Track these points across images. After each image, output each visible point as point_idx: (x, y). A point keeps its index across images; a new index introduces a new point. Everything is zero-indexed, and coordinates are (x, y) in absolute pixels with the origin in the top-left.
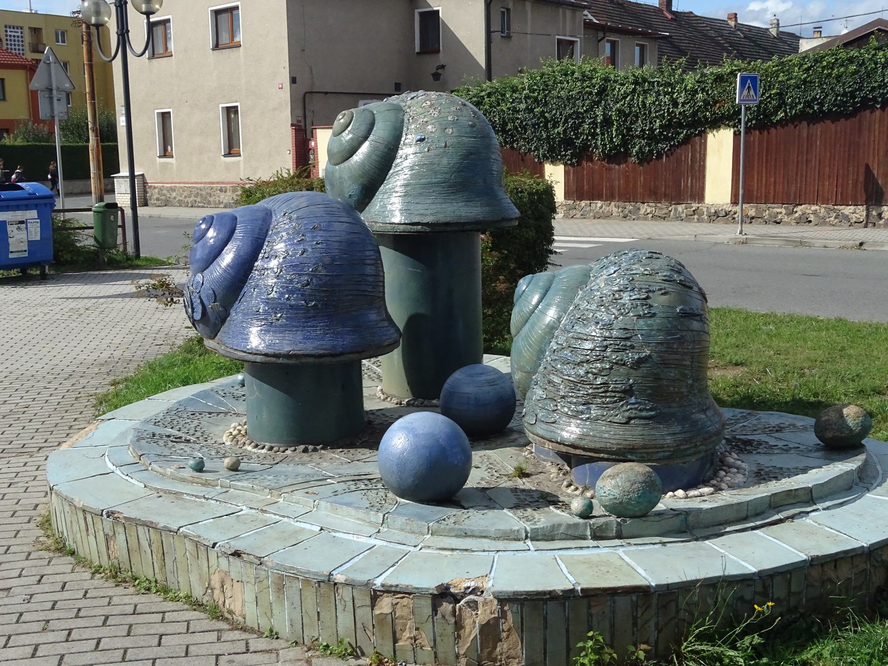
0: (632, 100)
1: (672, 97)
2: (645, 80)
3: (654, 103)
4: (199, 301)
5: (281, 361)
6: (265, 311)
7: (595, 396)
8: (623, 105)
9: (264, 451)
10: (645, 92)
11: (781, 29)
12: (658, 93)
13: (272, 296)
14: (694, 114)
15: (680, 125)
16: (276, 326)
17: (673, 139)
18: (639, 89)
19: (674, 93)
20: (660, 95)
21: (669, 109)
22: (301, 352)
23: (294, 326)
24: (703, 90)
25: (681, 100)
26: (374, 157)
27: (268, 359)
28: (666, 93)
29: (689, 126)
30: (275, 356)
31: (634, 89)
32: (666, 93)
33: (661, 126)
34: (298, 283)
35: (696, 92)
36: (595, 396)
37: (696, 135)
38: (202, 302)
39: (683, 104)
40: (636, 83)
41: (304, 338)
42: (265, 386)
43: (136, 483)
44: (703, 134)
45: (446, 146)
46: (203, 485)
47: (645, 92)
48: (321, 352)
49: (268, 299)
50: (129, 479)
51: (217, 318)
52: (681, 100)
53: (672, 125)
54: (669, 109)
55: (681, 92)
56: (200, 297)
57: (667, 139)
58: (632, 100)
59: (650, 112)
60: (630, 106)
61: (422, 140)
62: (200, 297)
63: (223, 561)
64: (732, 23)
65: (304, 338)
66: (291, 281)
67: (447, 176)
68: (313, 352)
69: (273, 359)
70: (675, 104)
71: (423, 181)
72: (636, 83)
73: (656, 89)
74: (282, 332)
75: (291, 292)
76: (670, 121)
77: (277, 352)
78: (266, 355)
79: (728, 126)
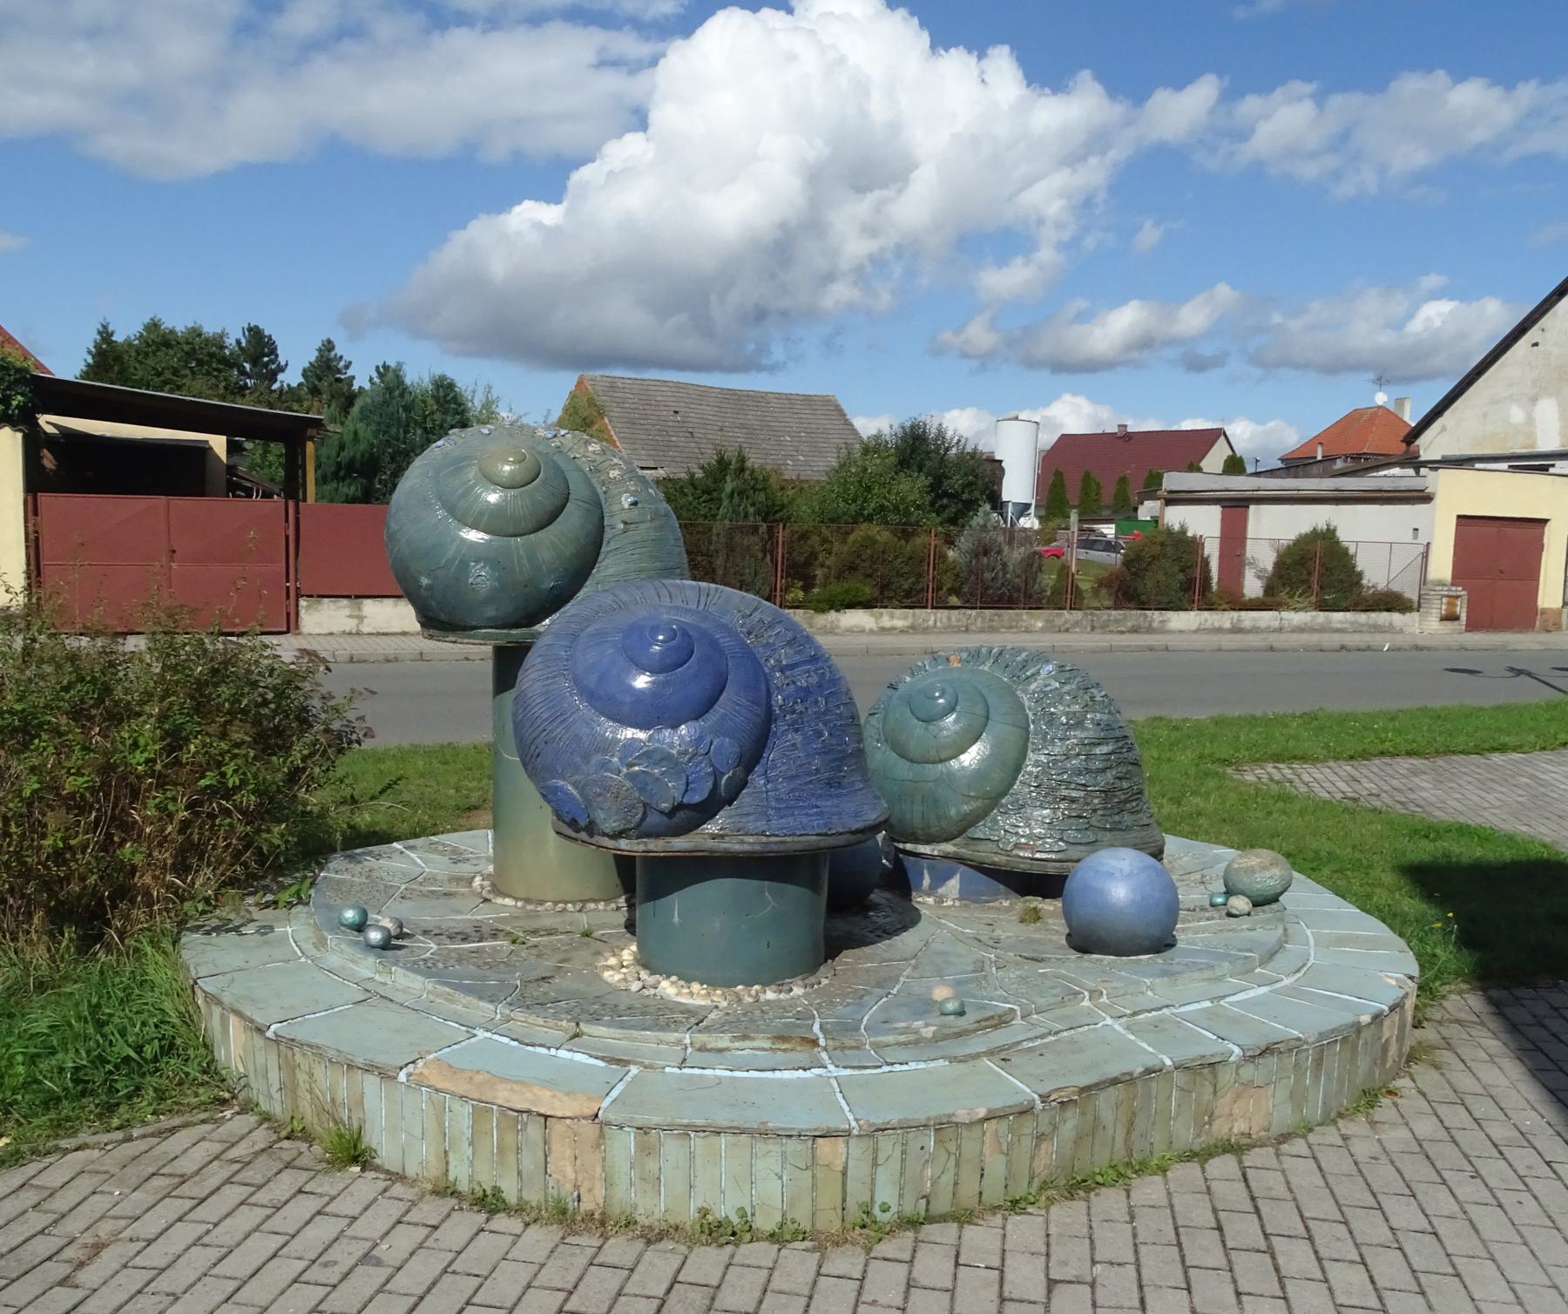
7: (1126, 801)
9: (798, 991)
36: (1126, 801)
43: (922, 1065)
46: (995, 1027)
50: (897, 1068)
61: (635, 504)
63: (1248, 1072)
78: (853, 833)
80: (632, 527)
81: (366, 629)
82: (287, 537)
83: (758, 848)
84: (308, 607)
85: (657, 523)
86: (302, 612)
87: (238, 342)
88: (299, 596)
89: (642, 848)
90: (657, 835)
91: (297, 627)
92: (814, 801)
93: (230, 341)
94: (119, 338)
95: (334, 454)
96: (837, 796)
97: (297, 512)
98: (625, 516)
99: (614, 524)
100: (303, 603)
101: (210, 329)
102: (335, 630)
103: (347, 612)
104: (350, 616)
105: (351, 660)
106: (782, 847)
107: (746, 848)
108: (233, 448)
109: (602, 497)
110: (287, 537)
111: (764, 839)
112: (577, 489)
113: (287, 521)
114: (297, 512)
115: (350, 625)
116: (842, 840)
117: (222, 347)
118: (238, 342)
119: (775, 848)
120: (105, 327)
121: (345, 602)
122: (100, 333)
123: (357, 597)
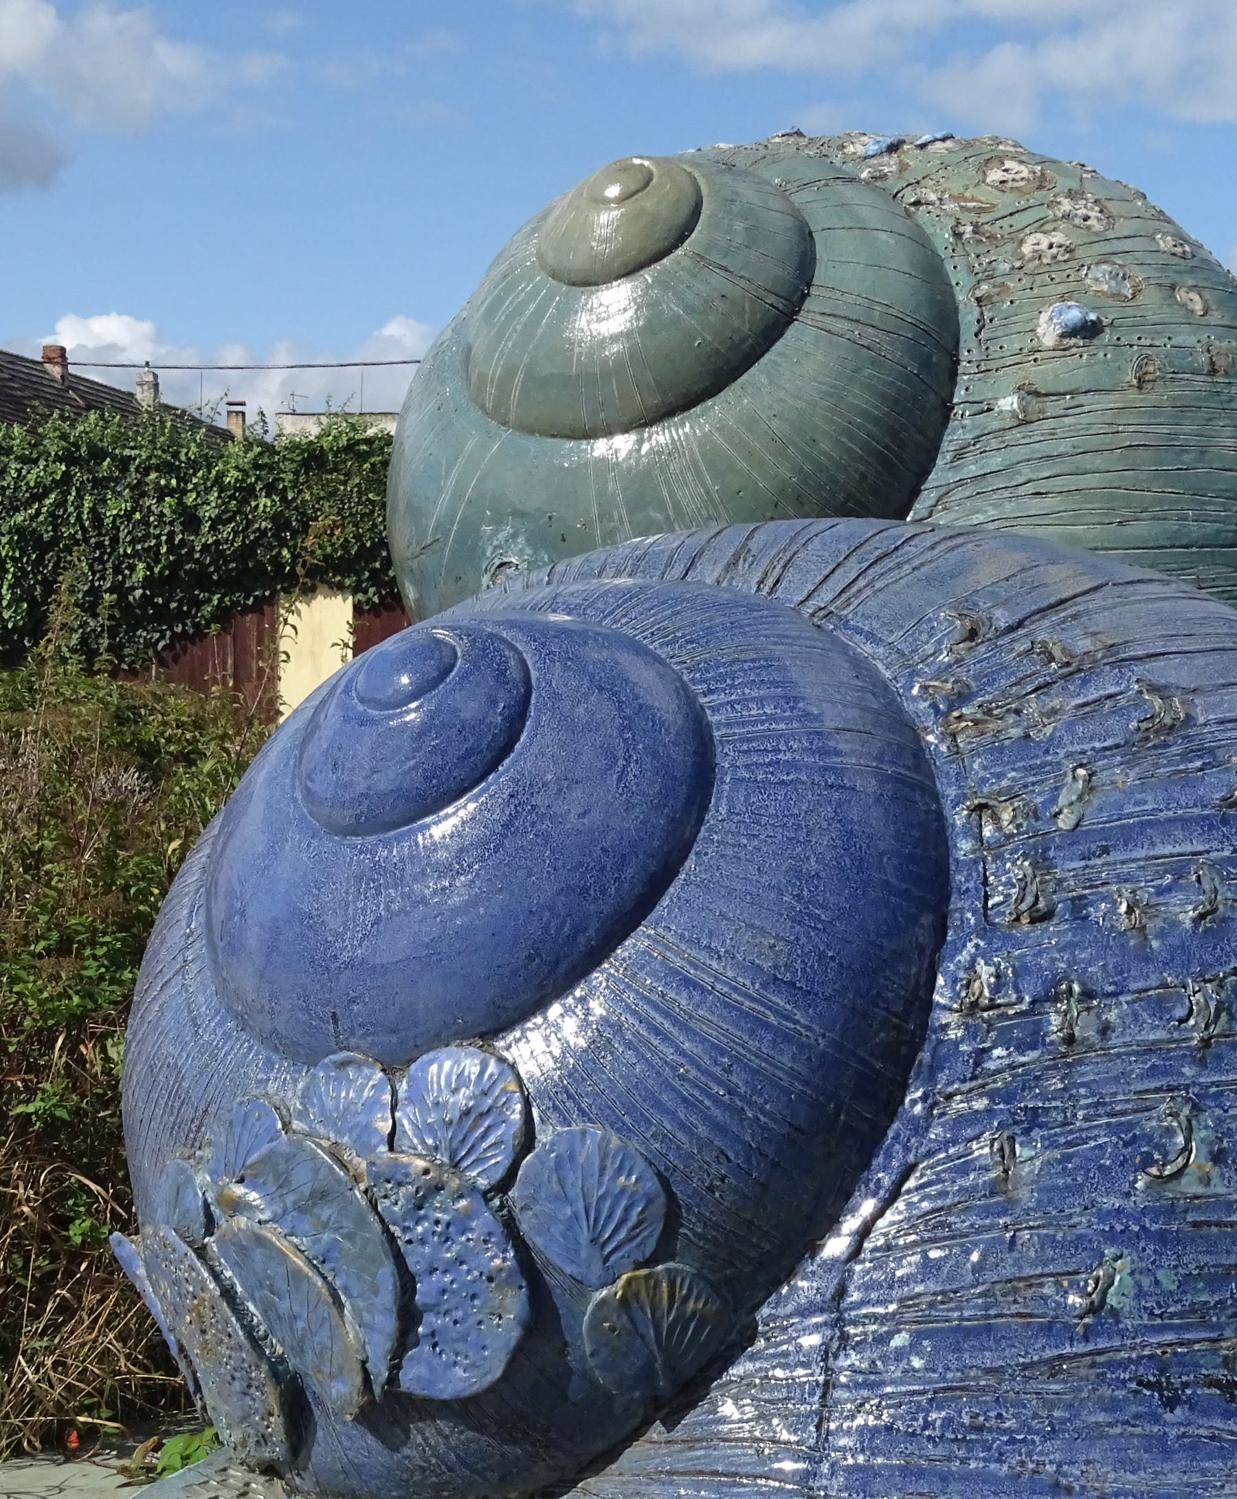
0: (61, 503)
1: (180, 502)
2: (97, 454)
3: (128, 515)
4: (501, 1259)
8: (33, 518)
10: (100, 484)
11: (165, 399)
12: (139, 491)
13: (1190, 1185)
14: (247, 551)
15: (201, 580)
17: (180, 616)
18: (78, 475)
19: (185, 492)
20: (144, 494)
21: (171, 535)
24: (270, 489)
25: (209, 512)
26: (860, 398)
29: (228, 584)
31: (67, 477)
33: (147, 582)
35: (250, 492)
37: (246, 610)
38: (529, 1268)
39: (216, 523)
40: (69, 458)
44: (265, 606)
45: (1213, 371)
47: (100, 484)
49: (1170, 1211)
51: (646, 1374)
52: (209, 512)
53: (180, 579)
54: (171, 535)
55: (208, 491)
56: (510, 1226)
57: (164, 616)
59: (115, 540)
60: (55, 520)
61: (1088, 331)
62: (510, 1226)
70: (191, 521)
71: (1141, 529)
72: (69, 458)
73: (133, 477)
76: (174, 567)
79: (340, 587)
80: (1052, 406)
85: (1159, 395)
99: (990, 395)
109: (968, 316)
112: (857, 274)
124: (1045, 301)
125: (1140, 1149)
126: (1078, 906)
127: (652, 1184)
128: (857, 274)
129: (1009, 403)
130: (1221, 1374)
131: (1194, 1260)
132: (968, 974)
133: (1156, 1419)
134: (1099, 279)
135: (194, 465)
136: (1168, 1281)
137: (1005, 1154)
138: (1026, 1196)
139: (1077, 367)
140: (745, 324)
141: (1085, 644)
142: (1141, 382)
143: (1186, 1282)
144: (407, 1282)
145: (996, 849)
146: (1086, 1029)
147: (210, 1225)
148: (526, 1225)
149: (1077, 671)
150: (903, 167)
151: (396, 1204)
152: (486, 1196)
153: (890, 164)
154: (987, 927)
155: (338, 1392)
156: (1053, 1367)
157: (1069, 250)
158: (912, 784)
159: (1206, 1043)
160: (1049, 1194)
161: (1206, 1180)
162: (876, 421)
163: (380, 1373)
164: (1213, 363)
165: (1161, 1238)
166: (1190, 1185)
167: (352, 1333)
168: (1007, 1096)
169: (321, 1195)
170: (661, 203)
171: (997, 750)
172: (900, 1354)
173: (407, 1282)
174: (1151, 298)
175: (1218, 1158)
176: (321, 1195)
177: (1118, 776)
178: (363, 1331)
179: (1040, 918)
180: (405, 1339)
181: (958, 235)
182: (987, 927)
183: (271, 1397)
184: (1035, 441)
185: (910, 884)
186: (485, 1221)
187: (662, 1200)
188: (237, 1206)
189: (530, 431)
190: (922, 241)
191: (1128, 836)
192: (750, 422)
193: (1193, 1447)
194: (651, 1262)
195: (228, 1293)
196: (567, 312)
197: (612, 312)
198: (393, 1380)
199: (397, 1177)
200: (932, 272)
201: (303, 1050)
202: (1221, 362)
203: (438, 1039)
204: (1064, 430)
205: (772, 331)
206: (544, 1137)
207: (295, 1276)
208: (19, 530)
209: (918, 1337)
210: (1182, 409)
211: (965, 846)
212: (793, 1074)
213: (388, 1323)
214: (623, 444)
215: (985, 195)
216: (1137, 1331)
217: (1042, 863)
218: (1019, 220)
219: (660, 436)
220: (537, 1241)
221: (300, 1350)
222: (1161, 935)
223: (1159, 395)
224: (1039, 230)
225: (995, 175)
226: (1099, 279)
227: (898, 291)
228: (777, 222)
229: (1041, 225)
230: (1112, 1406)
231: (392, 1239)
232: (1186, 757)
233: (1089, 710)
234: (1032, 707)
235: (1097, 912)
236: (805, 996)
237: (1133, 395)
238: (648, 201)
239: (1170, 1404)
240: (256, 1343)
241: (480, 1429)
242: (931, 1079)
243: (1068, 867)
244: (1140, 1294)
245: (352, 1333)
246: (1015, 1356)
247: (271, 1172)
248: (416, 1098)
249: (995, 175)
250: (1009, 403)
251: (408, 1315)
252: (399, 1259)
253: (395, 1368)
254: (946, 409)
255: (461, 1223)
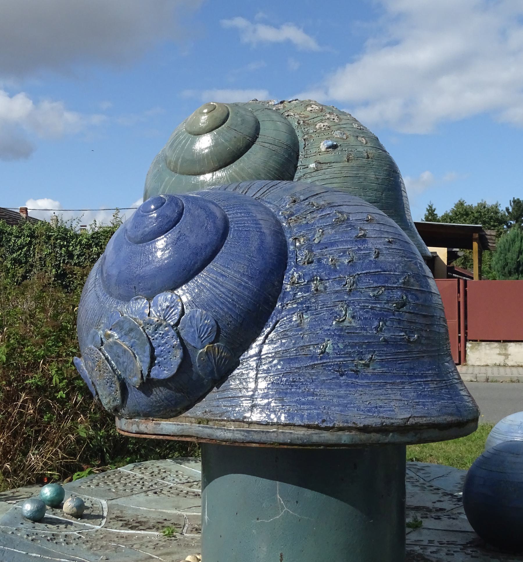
0: (28, 250)
1: (67, 249)
4: (176, 342)
5: (390, 437)
6: (338, 353)
8: (19, 255)
13: (346, 323)
16: (366, 377)
19: (69, 246)
20: (55, 247)
21: (64, 260)
22: (423, 421)
23: (394, 376)
25: (77, 252)
26: (272, 163)
27: (364, 437)
28: (61, 247)
30: (383, 429)
31: (30, 242)
32: (61, 247)
34: (388, 302)
38: (183, 344)
39: (79, 256)
41: (419, 396)
42: (308, 494)
45: (368, 158)
48: (449, 419)
49: (341, 330)
51: (212, 372)
52: (77, 252)
54: (64, 260)
55: (76, 246)
58: (28, 250)
61: (334, 147)
64: (24, 215)
65: (419, 396)
66: (377, 297)
67: (379, 194)
68: (441, 419)
69: (375, 437)
70: (71, 255)
73: (52, 241)
74: (381, 386)
75: (382, 316)
77: (388, 422)
78: (365, 429)
80: (324, 166)
81: (510, 363)
82: (459, 303)
83: (238, 436)
84: (472, 348)
85: (354, 163)
86: (468, 351)
87: (507, 209)
88: (466, 340)
89: (134, 428)
90: (147, 415)
91: (465, 360)
92: (311, 388)
93: (502, 209)
94: (440, 213)
95: (515, 257)
96: (354, 385)
97: (465, 286)
98: (319, 158)
100: (469, 345)
101: (490, 203)
102: (489, 362)
103: (498, 351)
104: (499, 354)
105: (487, 380)
106: (264, 438)
107: (229, 435)
108: (452, 256)
109: (301, 144)
110: (459, 303)
111: (246, 427)
113: (459, 292)
114: (465, 286)
115: (499, 360)
116: (345, 437)
117: (496, 213)
118: (507, 209)
119: (256, 437)
120: (430, 207)
121: (496, 344)
122: (428, 210)
123: (505, 341)
124: (322, 139)
125: (334, 315)
126: (319, 260)
127: (213, 322)
128: (271, 132)
129: (312, 165)
130: (354, 368)
131: (347, 341)
132: (293, 274)
133: (338, 378)
134: (337, 134)
135: (72, 237)
136: (341, 346)
137: (301, 317)
138: (306, 327)
139: (332, 156)
140: (241, 144)
141: (323, 203)
142: (348, 160)
143: (345, 346)
144: (153, 349)
145: (299, 248)
146: (321, 288)
147: (102, 344)
148: (182, 334)
149: (320, 208)
150: (284, 107)
151: (150, 330)
152: (173, 327)
153: (281, 106)
154: (297, 265)
155: (135, 380)
156: (312, 367)
157: (329, 127)
158: (279, 233)
159: (350, 290)
160: (312, 327)
161: (350, 323)
162: (277, 170)
163: (146, 373)
164: (368, 156)
165: (339, 336)
166: (346, 323)
167: (138, 364)
168: (302, 303)
169: (131, 330)
170: (218, 114)
171: (300, 226)
172: (275, 365)
173: (153, 349)
174: (352, 139)
175: (353, 317)
176: (131, 330)
177: (330, 231)
178: (141, 364)
179: (309, 263)
180: (152, 364)
181: (299, 123)
182: (297, 265)
183: (117, 386)
184: (320, 175)
185: (279, 260)
186: (172, 332)
187: (216, 326)
188: (110, 336)
189: (183, 174)
190: (290, 125)
191: (332, 244)
192: (242, 169)
193: (347, 385)
194: (213, 343)
195: (107, 359)
196: (193, 143)
197: (204, 143)
198: (149, 375)
199: (150, 323)
200: (292, 132)
201: (126, 298)
202: (370, 155)
203: (161, 291)
204: (328, 172)
205: (248, 146)
206: (187, 311)
207: (125, 351)
208: (14, 259)
209: (279, 361)
210: (360, 167)
211: (291, 248)
212: (248, 297)
213: (148, 360)
214: (208, 177)
215: (306, 113)
216: (333, 358)
217: (311, 251)
218: (315, 120)
219: (219, 174)
220: (185, 338)
221: (125, 371)
222: (339, 266)
223: (354, 163)
224: (321, 122)
225: (309, 109)
226: (337, 134)
227: (284, 137)
228: (249, 118)
229: (321, 121)
230: (328, 375)
231: (149, 339)
232: (347, 227)
233: (322, 217)
234: (309, 217)
235: (324, 261)
236: (251, 278)
237: (346, 163)
238: (215, 113)
239: (342, 375)
240: (114, 371)
241: (170, 389)
242: (283, 300)
243: (317, 252)
244: (334, 349)
245: (138, 364)
246: (303, 364)
247: (118, 326)
248: (156, 305)
249: (309, 109)
250: (312, 165)
251: (153, 358)
252: (151, 344)
253: (149, 372)
254: (296, 167)
255: (166, 334)
